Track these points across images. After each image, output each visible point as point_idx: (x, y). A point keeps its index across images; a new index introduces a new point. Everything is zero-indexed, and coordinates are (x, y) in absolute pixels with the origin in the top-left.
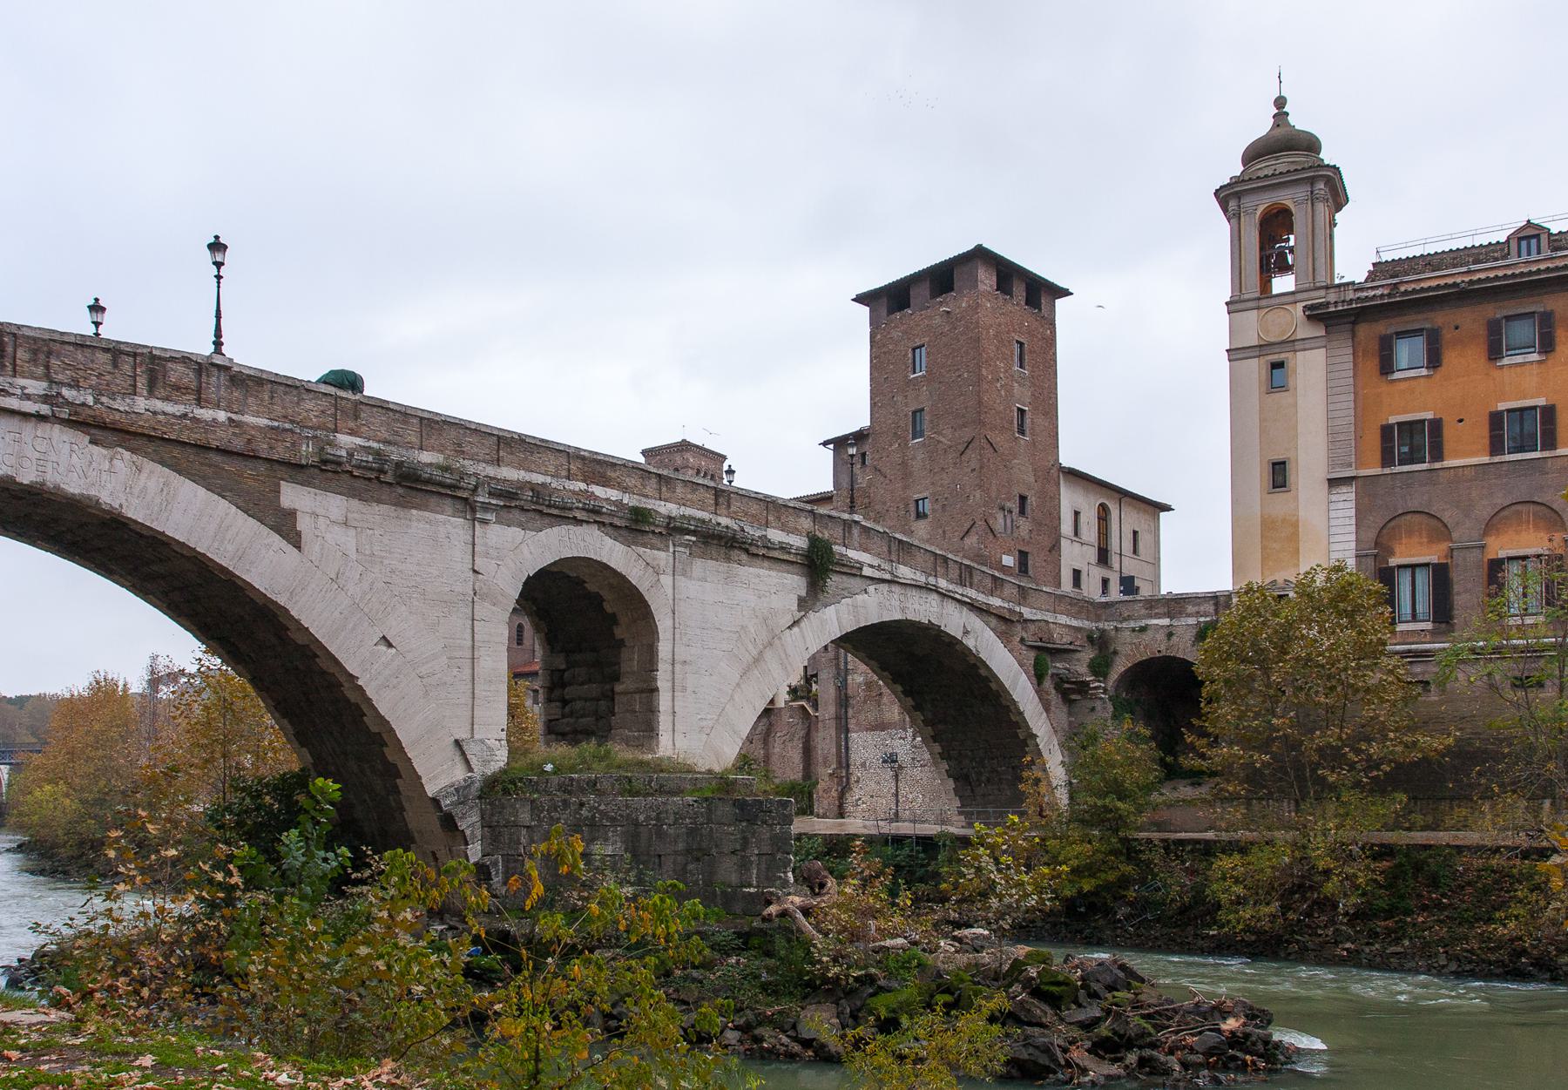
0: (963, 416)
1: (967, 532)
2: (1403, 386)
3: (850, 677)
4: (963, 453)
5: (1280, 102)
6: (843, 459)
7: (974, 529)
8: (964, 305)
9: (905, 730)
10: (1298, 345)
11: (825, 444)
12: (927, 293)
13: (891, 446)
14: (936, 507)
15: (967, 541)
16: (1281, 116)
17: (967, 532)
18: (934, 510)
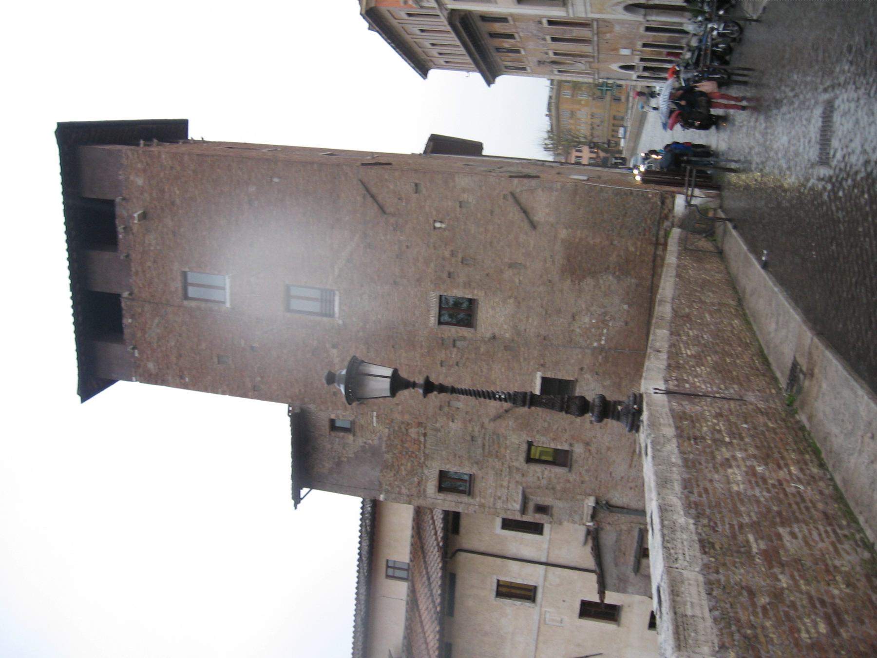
1: (525, 212)
4: (382, 208)
7: (524, 198)
8: (140, 182)
11: (297, 498)
12: (107, 255)
14: (462, 279)
15: (541, 215)
17: (525, 212)
18: (468, 285)
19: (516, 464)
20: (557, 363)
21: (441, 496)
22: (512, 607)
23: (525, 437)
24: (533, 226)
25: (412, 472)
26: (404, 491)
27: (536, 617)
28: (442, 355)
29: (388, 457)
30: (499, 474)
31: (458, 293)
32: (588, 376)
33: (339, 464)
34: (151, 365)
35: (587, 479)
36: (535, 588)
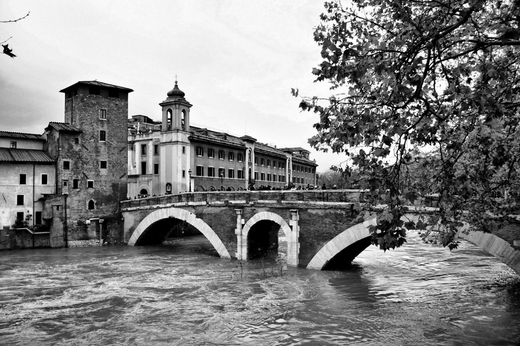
0: (122, 139)
2: (199, 158)
3: (68, 221)
4: (121, 151)
5: (176, 82)
6: (66, 138)
7: (125, 176)
9: (99, 239)
10: (187, 144)
13: (91, 139)
14: (110, 165)
16: (176, 86)
18: (109, 166)
19: (73, 177)
20: (96, 184)
21: (63, 162)
22: (18, 178)
23: (80, 179)
24: (120, 178)
25: (68, 156)
26: (63, 154)
27: (16, 185)
28: (95, 162)
29: (71, 150)
30: (70, 174)
31: (107, 165)
32: (94, 190)
33: (68, 140)
34: (85, 99)
35: (72, 192)
36: (25, 184)
